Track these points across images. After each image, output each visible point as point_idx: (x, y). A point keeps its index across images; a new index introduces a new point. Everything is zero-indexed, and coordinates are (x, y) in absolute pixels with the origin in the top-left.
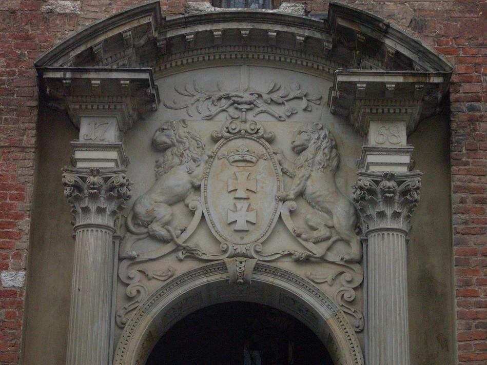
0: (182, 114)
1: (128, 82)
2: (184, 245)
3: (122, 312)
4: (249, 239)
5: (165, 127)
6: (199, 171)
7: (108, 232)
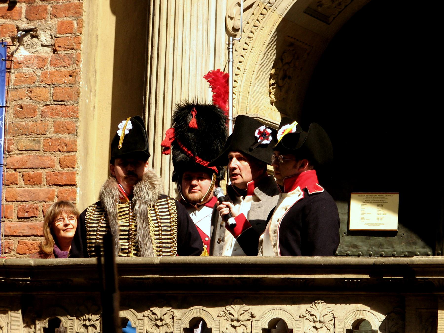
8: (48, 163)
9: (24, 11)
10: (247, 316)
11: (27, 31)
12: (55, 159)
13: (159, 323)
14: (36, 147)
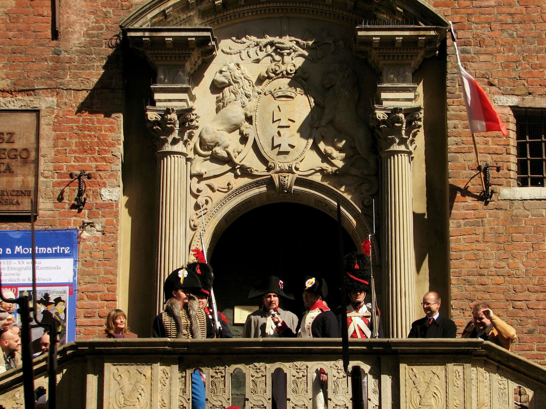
0: (236, 58)
1: (194, 39)
2: (240, 164)
3: (195, 217)
4: (289, 158)
5: (224, 69)
6: (251, 105)
7: (182, 156)
8: (101, 289)
9: (87, 214)
10: (305, 367)
11: (88, 224)
12: (105, 288)
13: (258, 371)
14: (94, 281)
